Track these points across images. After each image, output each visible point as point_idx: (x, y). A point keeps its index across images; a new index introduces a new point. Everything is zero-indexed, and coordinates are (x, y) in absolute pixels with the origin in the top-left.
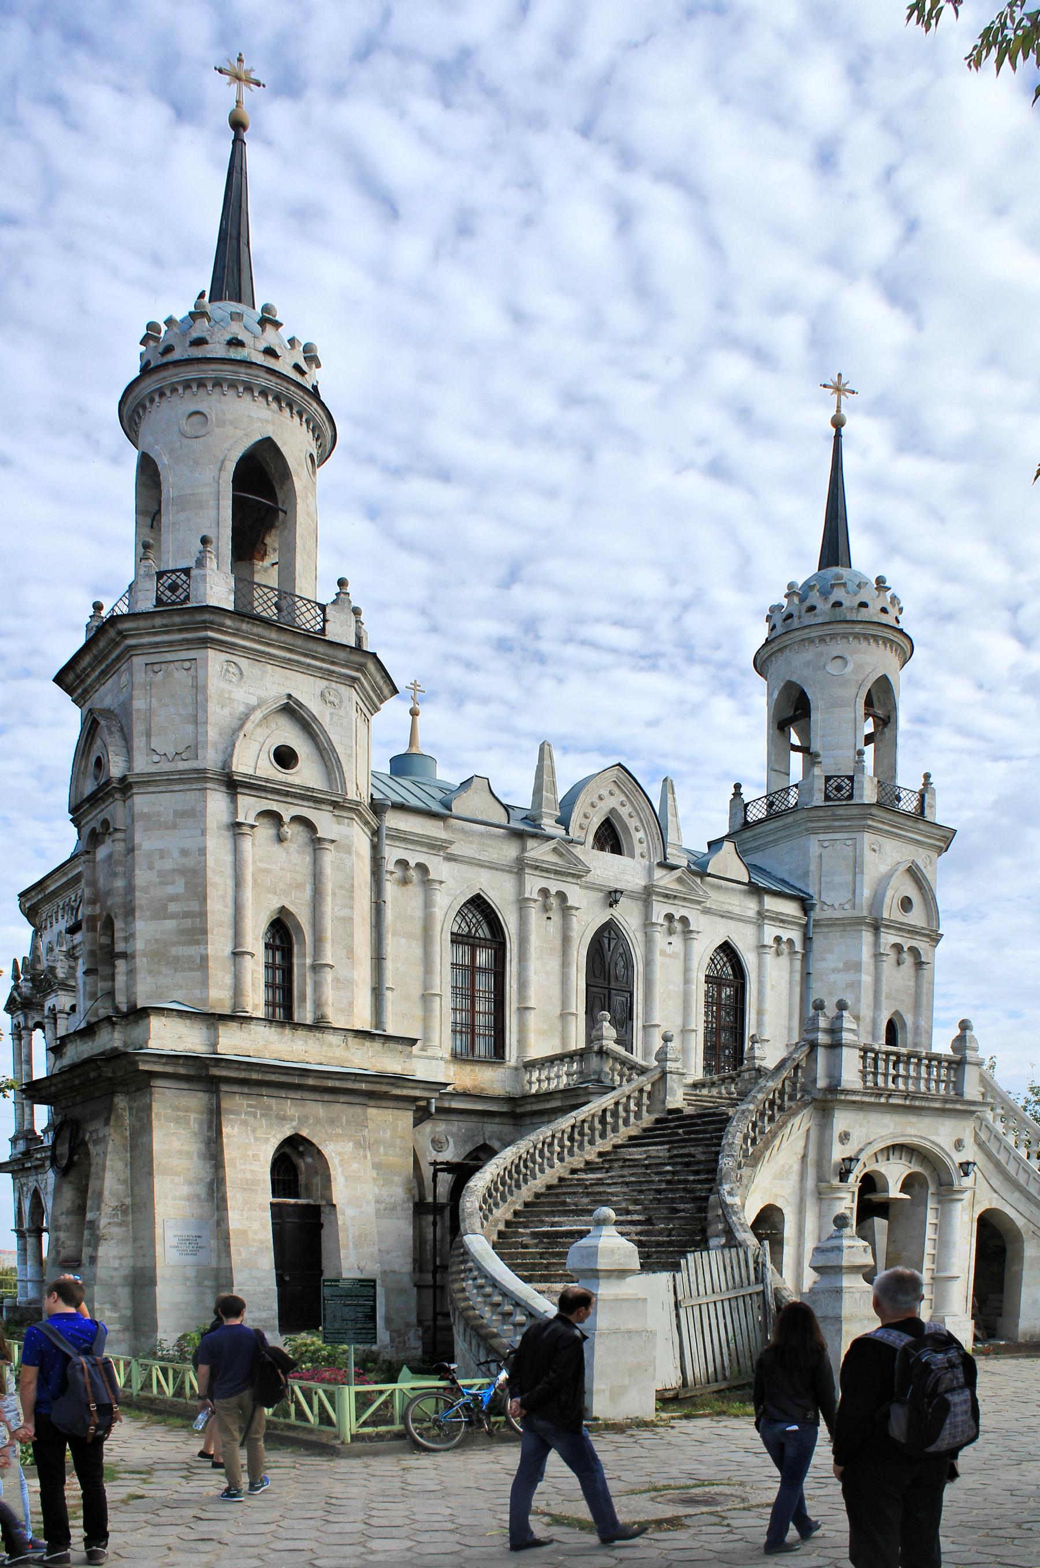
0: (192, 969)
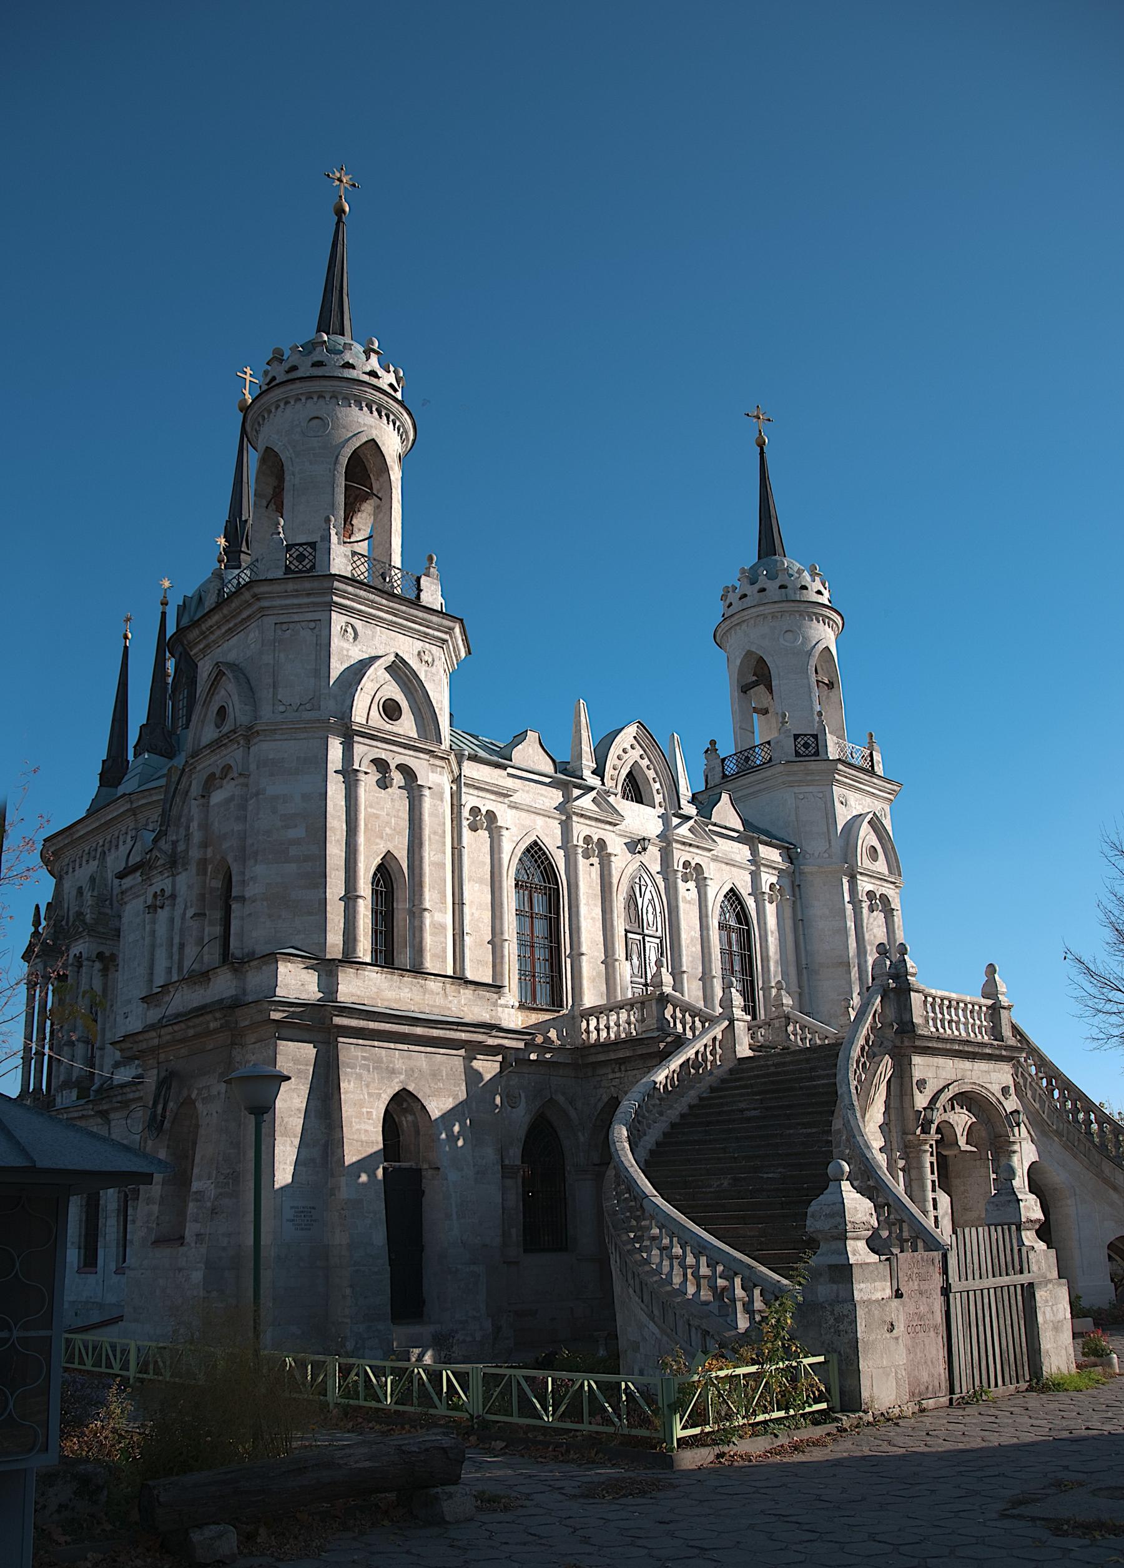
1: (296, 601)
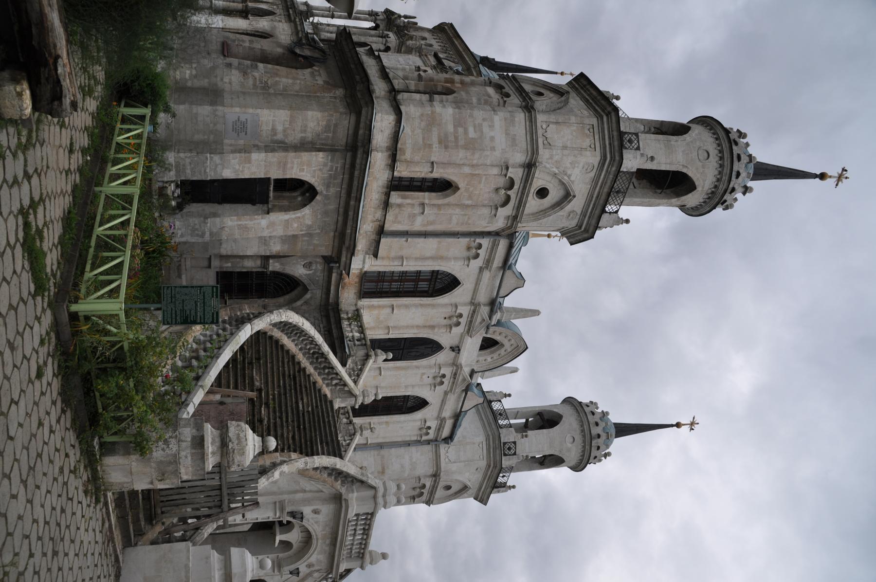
0: (424, 139)
1: (607, 137)
